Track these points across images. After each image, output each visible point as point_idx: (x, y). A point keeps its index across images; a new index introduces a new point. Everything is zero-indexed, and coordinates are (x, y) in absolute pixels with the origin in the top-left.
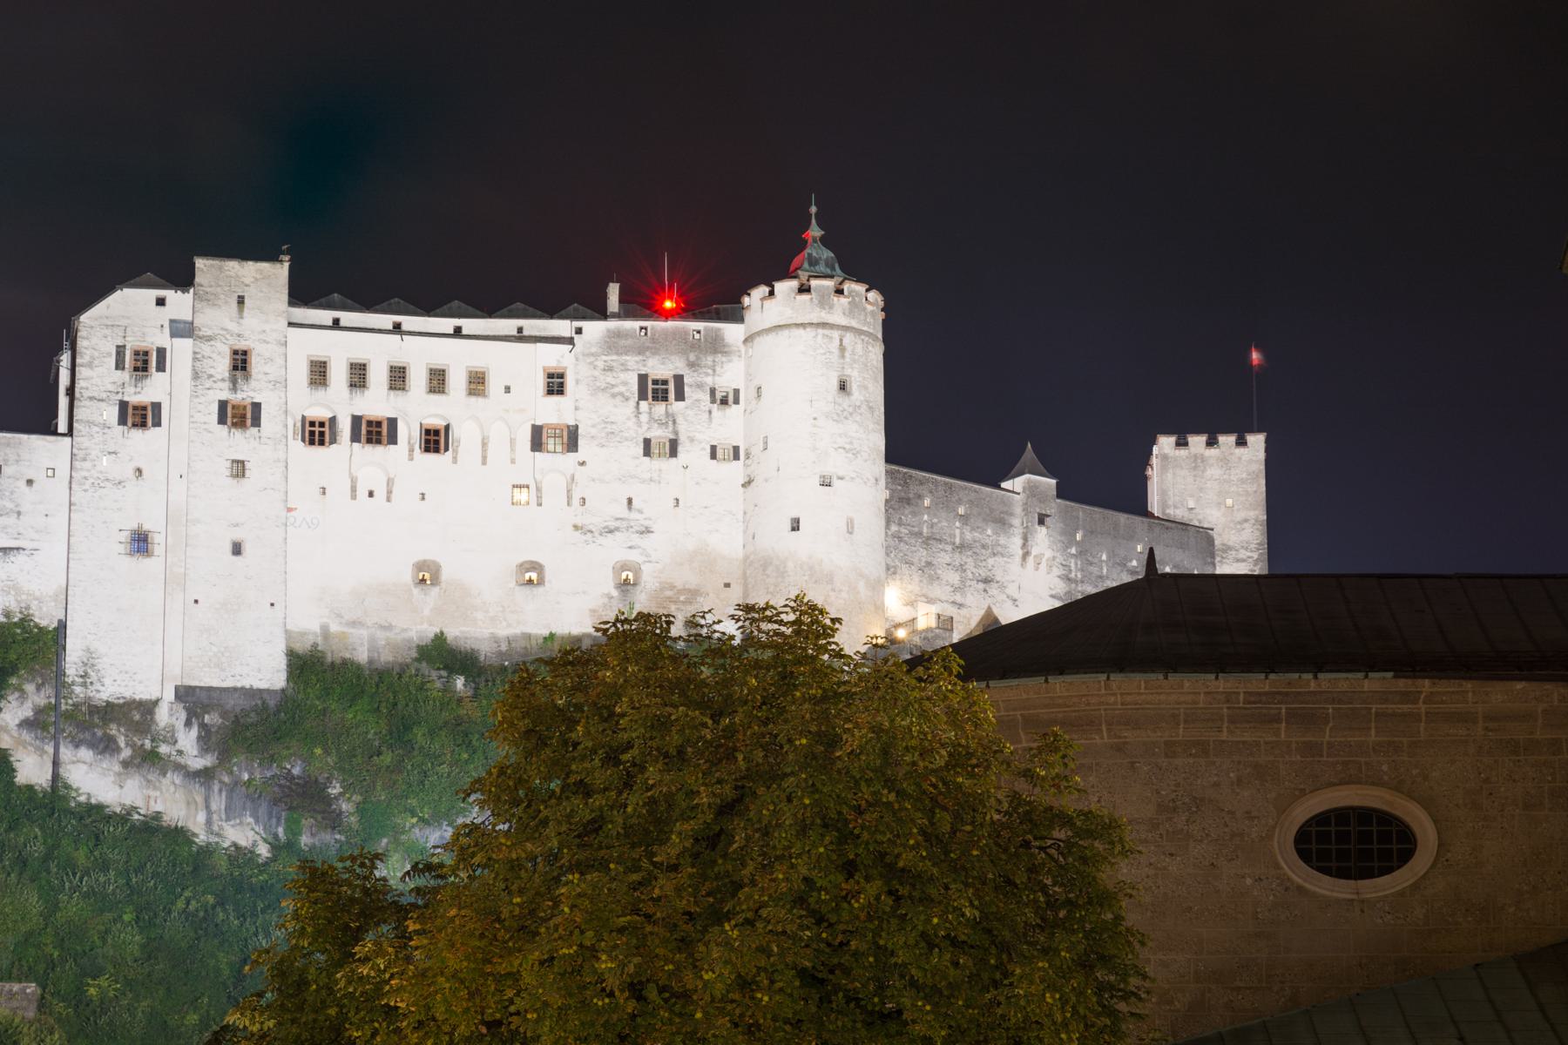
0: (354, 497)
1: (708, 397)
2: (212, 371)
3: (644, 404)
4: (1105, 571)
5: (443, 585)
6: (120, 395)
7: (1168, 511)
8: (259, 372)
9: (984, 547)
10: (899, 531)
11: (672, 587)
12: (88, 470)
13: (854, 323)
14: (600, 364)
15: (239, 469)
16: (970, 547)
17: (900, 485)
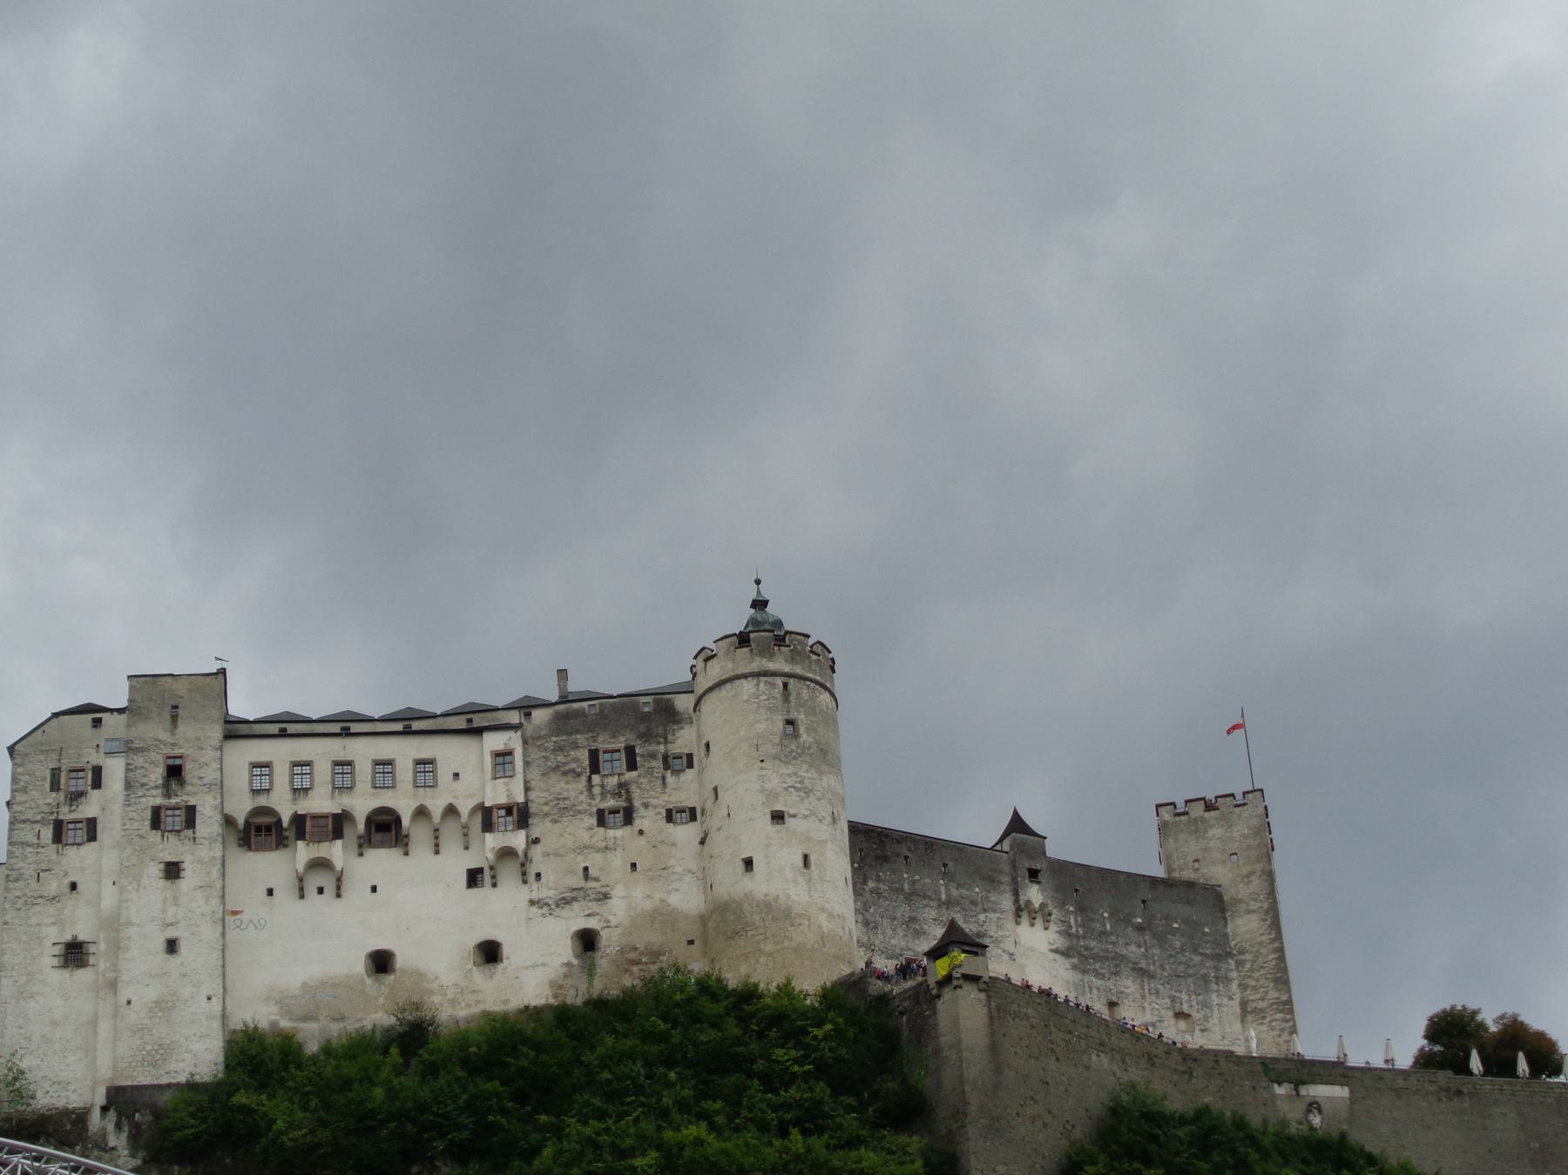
0: (302, 897)
1: (658, 764)
2: (145, 780)
3: (596, 779)
4: (1108, 927)
5: (398, 973)
6: (55, 814)
7: (1173, 875)
8: (194, 777)
9: (973, 903)
10: (878, 888)
11: (635, 949)
12: (21, 889)
13: (798, 670)
14: (550, 745)
15: (173, 871)
16: (957, 903)
17: (875, 843)
